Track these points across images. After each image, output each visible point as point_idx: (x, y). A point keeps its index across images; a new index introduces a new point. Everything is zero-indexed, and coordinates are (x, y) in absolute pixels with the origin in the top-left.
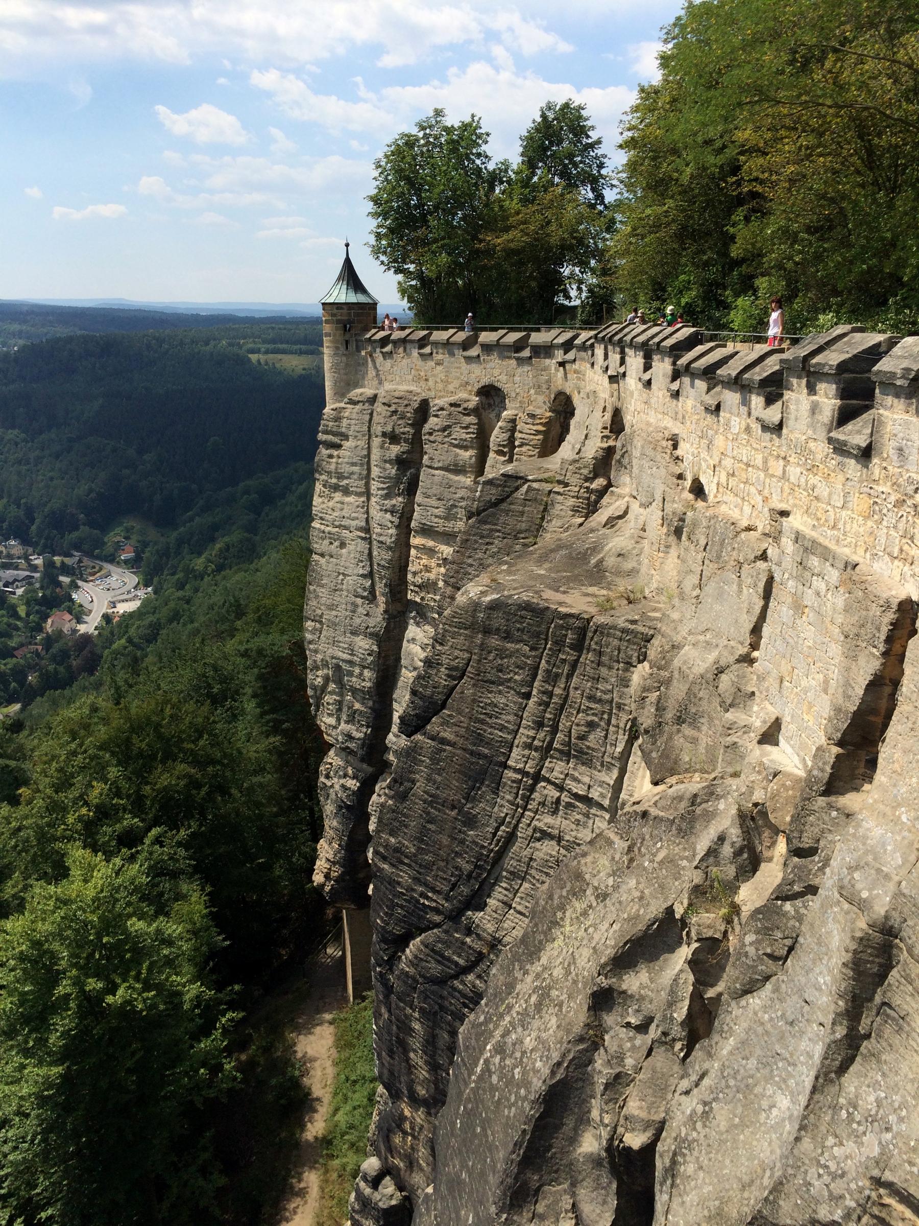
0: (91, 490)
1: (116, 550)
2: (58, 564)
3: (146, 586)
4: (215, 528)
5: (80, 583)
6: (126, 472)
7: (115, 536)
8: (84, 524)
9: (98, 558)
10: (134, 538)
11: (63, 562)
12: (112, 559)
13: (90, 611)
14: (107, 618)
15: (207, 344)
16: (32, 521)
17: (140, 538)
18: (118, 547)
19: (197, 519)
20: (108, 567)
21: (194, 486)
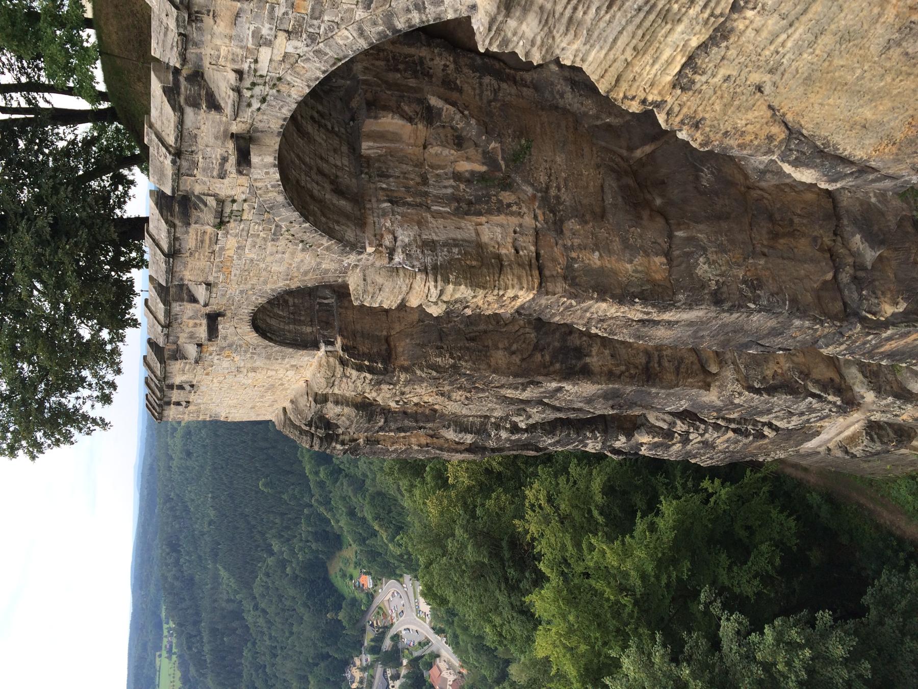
0: (305, 605)
1: (363, 590)
2: (373, 644)
3: (401, 576)
4: (352, 513)
5: (392, 632)
6: (288, 570)
7: (347, 588)
8: (337, 614)
9: (369, 605)
10: (351, 570)
11: (372, 640)
12: (371, 596)
13: (426, 638)
14: (439, 631)
15: (171, 458)
16: (328, 656)
17: (352, 565)
18: (360, 588)
19: (342, 524)
21: (306, 511)
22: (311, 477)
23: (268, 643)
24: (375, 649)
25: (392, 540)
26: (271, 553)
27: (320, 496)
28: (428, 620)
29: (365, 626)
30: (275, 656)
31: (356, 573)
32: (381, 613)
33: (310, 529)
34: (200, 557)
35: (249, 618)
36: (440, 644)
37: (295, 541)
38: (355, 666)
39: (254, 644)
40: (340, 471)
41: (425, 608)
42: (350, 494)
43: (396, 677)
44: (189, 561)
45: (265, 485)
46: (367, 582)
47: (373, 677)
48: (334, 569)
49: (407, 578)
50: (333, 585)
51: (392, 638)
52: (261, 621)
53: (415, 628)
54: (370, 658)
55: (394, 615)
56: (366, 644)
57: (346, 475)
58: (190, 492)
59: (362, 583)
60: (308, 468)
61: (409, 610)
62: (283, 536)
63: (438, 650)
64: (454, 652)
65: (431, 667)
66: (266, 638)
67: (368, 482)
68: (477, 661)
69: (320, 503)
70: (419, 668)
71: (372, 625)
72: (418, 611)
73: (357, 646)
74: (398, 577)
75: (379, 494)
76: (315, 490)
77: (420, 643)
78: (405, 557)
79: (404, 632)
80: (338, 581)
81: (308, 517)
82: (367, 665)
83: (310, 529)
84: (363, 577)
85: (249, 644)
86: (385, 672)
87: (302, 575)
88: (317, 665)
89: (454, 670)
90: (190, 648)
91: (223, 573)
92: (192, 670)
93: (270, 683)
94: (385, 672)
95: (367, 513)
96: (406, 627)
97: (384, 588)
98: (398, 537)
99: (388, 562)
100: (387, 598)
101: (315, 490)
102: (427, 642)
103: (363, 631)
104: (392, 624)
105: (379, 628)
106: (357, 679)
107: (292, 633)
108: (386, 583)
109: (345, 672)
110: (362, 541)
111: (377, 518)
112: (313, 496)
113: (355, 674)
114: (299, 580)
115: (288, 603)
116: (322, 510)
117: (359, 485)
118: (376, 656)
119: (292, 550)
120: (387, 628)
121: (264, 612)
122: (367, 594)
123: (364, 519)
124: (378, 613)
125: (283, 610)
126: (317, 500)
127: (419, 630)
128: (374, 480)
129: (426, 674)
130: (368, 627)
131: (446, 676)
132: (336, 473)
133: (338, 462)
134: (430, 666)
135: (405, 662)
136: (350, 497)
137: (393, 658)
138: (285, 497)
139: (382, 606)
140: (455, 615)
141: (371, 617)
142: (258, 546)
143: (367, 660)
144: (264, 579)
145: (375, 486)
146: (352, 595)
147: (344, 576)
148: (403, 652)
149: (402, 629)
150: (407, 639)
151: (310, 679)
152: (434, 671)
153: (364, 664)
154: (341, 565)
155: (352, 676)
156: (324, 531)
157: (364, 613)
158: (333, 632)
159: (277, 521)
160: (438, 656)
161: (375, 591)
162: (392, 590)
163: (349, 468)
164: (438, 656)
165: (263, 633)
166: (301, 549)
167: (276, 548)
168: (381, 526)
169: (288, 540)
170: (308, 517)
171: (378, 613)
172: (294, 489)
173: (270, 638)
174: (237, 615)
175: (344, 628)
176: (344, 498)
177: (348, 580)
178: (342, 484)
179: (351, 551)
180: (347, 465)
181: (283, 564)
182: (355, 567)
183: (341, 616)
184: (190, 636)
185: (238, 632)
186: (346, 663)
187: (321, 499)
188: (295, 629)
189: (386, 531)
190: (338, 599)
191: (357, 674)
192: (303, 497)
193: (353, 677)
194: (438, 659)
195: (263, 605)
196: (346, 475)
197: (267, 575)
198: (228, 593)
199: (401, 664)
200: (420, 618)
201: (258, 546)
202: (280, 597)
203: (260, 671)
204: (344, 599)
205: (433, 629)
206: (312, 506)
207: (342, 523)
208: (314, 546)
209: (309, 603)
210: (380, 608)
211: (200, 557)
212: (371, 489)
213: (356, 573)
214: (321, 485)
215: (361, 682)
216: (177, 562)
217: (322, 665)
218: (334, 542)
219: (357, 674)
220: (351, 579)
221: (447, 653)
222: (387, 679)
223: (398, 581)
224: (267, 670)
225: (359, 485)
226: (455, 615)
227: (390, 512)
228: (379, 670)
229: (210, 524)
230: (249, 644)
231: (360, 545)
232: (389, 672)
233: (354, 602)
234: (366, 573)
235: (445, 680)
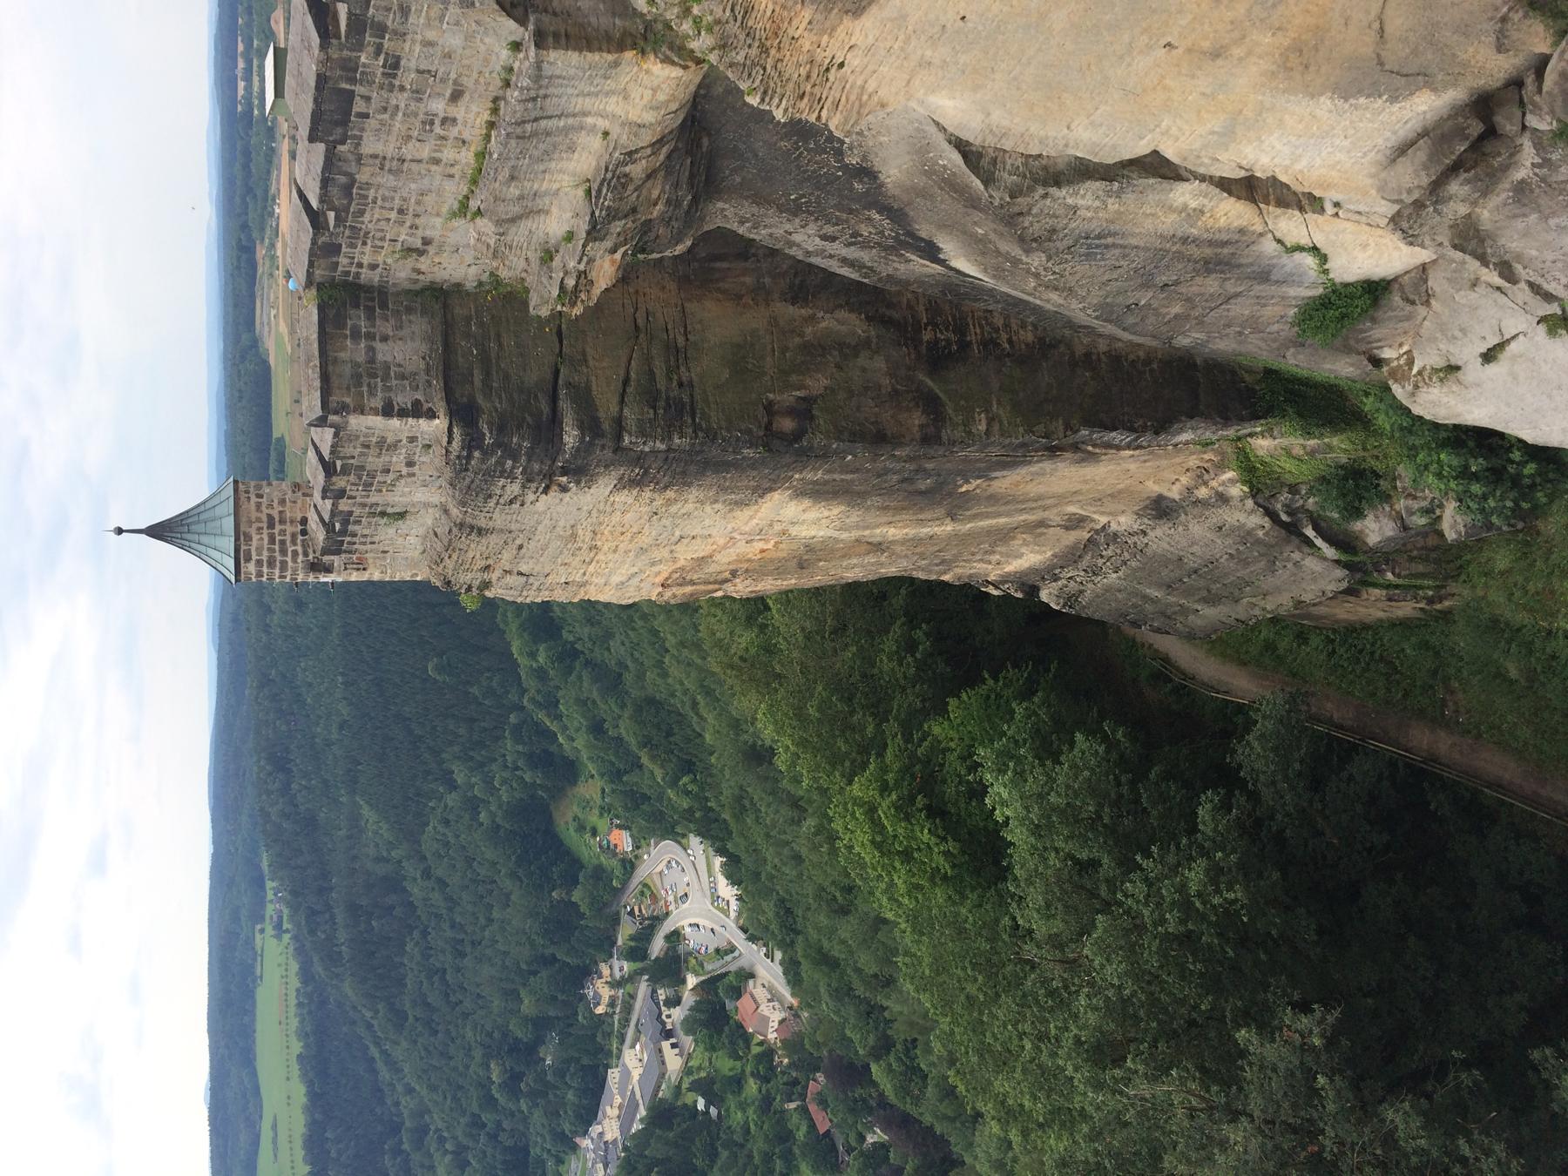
0: (513, 875)
1: (615, 854)
2: (633, 944)
4: (597, 729)
5: (667, 927)
6: (483, 816)
7: (587, 849)
8: (569, 893)
10: (593, 819)
11: (632, 938)
12: (629, 865)
13: (730, 943)
15: (269, 611)
16: (554, 959)
17: (596, 811)
18: (610, 850)
20: (641, 874)
21: (513, 719)
22: (523, 661)
23: (449, 933)
24: (637, 951)
25: (674, 783)
26: (453, 786)
27: (538, 691)
28: (733, 915)
29: (618, 913)
30: (462, 955)
31: (603, 825)
32: (648, 893)
33: (520, 748)
34: (325, 782)
35: (416, 891)
36: (751, 954)
37: (494, 767)
38: (600, 977)
39: (425, 933)
40: (575, 654)
41: (727, 891)
42: (595, 695)
43: (674, 1002)
44: (306, 787)
45: (440, 669)
46: (623, 841)
47: (633, 997)
48: (565, 819)
49: (694, 841)
50: (561, 843)
51: (668, 938)
52: (436, 896)
53: (709, 925)
54: (626, 965)
55: (671, 898)
56: (620, 942)
57: (588, 663)
58: (305, 670)
59: (613, 842)
60: (515, 647)
61: (699, 894)
62: (472, 758)
63: (752, 966)
64: (789, 982)
65: (739, 996)
66: (446, 926)
67: (628, 678)
68: (837, 1012)
69: (539, 705)
70: (717, 994)
71: (632, 913)
72: (715, 898)
73: (606, 945)
74: (679, 839)
75: (651, 701)
76: (530, 683)
77: (717, 951)
78: (698, 815)
79: (688, 930)
80: (570, 835)
81: (517, 729)
82: (622, 977)
83: (520, 748)
84: (616, 832)
85: (416, 934)
86: (654, 992)
87: (507, 826)
88: (535, 973)
89: (782, 1005)
90: (312, 932)
91: (366, 812)
92: (318, 969)
93: (452, 999)
94: (654, 992)
95: (627, 730)
96: (693, 921)
97: (653, 853)
98: (685, 779)
99: (661, 811)
100: (658, 869)
101: (530, 683)
102: (732, 949)
103: (615, 921)
104: (667, 914)
105: (644, 919)
106: (605, 999)
107: (490, 921)
108: (656, 844)
109: (583, 988)
110: (615, 775)
111: (646, 743)
112: (524, 691)
113: (601, 991)
114: (502, 833)
115: (483, 872)
116: (541, 716)
117: (612, 681)
118: (639, 965)
119: (488, 782)
120: (657, 920)
121: (442, 883)
122: (623, 861)
123: (619, 739)
124: (642, 893)
125: (473, 881)
126: (532, 700)
127: (717, 928)
128: (641, 676)
129: (729, 1005)
130: (625, 918)
131: (766, 1013)
132: (568, 656)
133: (571, 638)
134: (737, 993)
135: (692, 981)
136: (594, 702)
137: (670, 969)
138: (475, 690)
139: (648, 881)
140: (798, 933)
141: (630, 899)
142: (428, 773)
143: (621, 969)
144: (440, 828)
145: (643, 687)
146: (595, 862)
147: (581, 828)
148: (686, 961)
149: (685, 923)
150: (694, 940)
151: (523, 993)
152: (744, 1003)
153: (618, 975)
154: (575, 808)
155: (596, 993)
156: (545, 751)
157: (618, 892)
158: (563, 922)
159: (462, 731)
160: (752, 976)
161: (636, 857)
162: (667, 858)
163: (592, 651)
164: (752, 976)
165: (438, 916)
166: (504, 782)
167: (460, 778)
168: (653, 758)
169: (482, 765)
170: (517, 729)
171: (642, 893)
172: (490, 678)
173: (453, 926)
174: (394, 884)
175: (582, 916)
176: (583, 703)
177: (587, 836)
178: (580, 678)
179: (591, 788)
180: (589, 645)
181: (473, 805)
182: (601, 815)
183: (577, 896)
184: (312, 913)
185: (398, 912)
186: (586, 972)
187: (539, 698)
188: (496, 914)
189: (662, 767)
190: (572, 866)
191: (606, 993)
192: (507, 692)
193: (597, 997)
194: (751, 982)
195: (439, 872)
196: (588, 663)
197: (447, 822)
198: (377, 845)
199: (684, 981)
200: (718, 908)
201: (428, 773)
202: (469, 861)
203: (436, 978)
204: (582, 866)
205: (744, 929)
206: (523, 708)
207: (576, 742)
208: (528, 777)
209: (521, 873)
210: (646, 885)
211: (325, 782)
212: (635, 693)
213: (603, 825)
214: (541, 674)
215: (612, 1004)
216: (285, 790)
217: (544, 974)
218: (566, 772)
219: (606, 993)
220: (594, 833)
221: (768, 971)
222: (657, 1004)
223: (679, 843)
224: (448, 977)
225: (612, 681)
226: (798, 933)
227: (669, 734)
228: (643, 988)
229: (341, 728)
230: (416, 934)
231: (612, 782)
232: (662, 994)
233: (600, 874)
234: (620, 827)
235: (766, 1020)
